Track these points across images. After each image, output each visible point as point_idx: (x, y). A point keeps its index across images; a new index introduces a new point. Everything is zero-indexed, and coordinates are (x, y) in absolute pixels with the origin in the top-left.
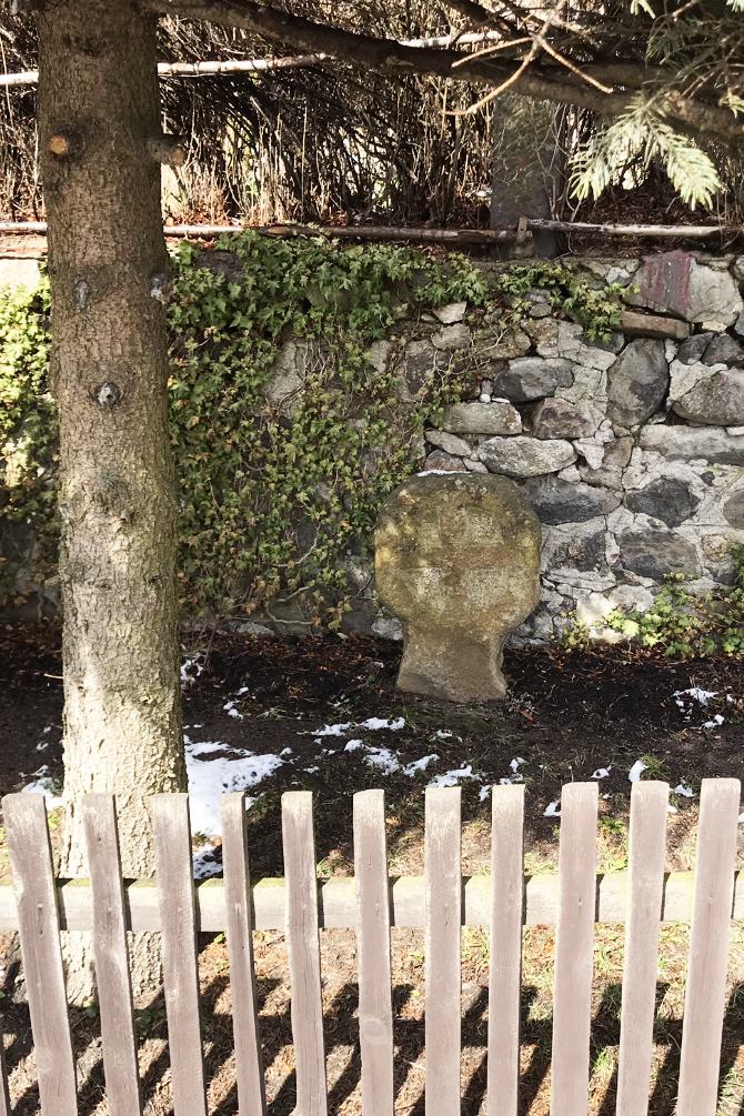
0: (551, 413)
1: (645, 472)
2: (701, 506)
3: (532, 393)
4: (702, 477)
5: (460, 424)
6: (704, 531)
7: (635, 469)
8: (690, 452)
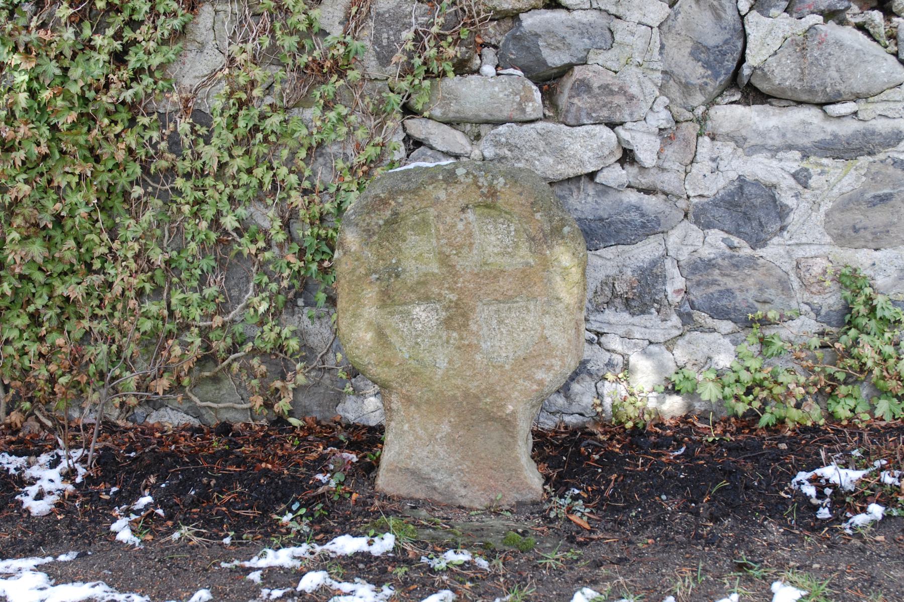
0: (584, 86)
1: (714, 171)
2: (793, 218)
3: (555, 59)
4: (794, 176)
5: (454, 107)
6: (799, 253)
7: (703, 166)
8: (778, 142)
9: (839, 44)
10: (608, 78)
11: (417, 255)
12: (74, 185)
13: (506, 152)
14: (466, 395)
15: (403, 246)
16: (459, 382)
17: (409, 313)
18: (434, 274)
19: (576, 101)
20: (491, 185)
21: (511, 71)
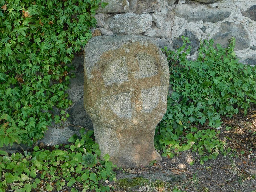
4: (201, 29)
8: (197, 17)
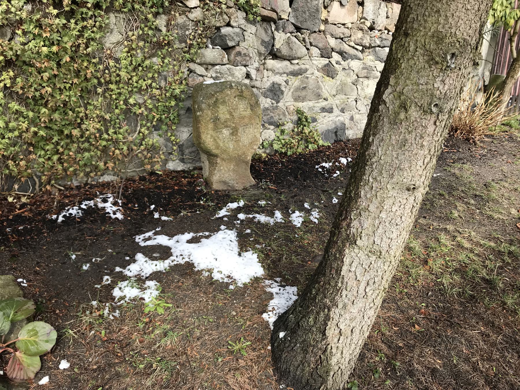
0: (239, 54)
1: (267, 80)
2: (285, 94)
3: (231, 44)
5: (203, 59)
6: (287, 104)
7: (265, 79)
8: (281, 71)
9: (295, 43)
10: (245, 51)
11: (223, 113)
12: (67, 88)
13: (219, 75)
14: (238, 155)
15: (218, 109)
16: (236, 152)
17: (221, 131)
18: (228, 119)
19: (237, 58)
20: (241, 89)
21: (218, 47)
